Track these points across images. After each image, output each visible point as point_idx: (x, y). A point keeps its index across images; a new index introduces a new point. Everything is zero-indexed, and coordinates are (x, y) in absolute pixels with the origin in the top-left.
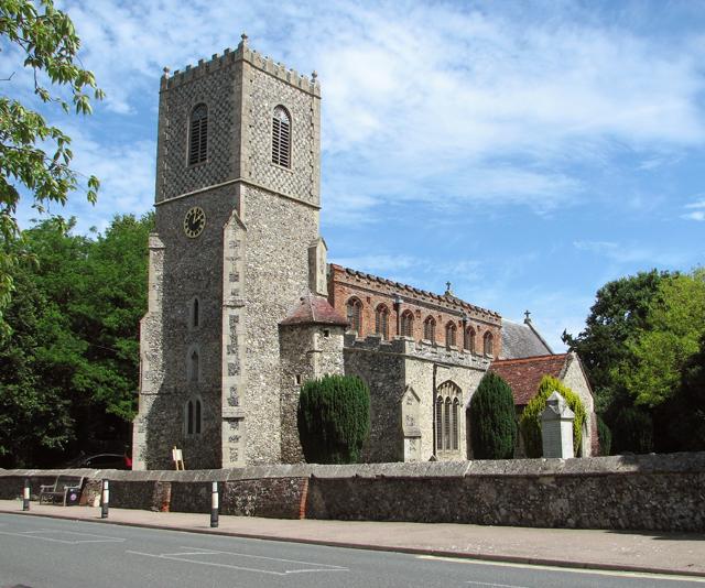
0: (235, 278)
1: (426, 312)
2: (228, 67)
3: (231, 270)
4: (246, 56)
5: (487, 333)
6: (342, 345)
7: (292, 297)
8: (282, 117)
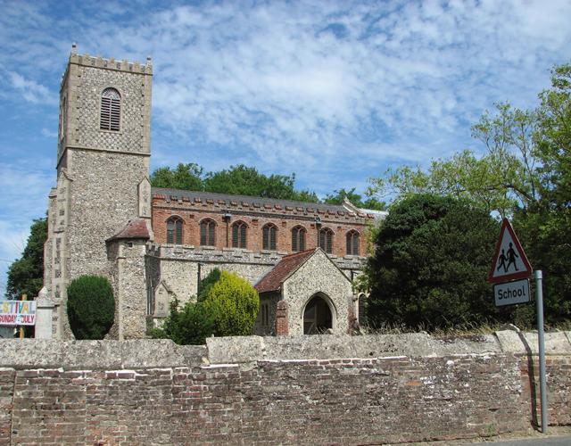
3: (60, 208)
8: (113, 95)
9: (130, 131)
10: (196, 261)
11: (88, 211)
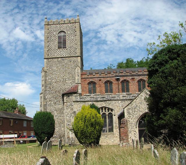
8: (62, 34)
9: (71, 47)
11: (53, 84)
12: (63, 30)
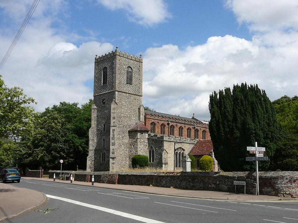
0: (114, 118)
1: (179, 125)
2: (111, 58)
4: (118, 53)
5: (204, 130)
6: (147, 137)
7: (133, 122)
8: (130, 70)
10: (174, 142)
12: (131, 66)
